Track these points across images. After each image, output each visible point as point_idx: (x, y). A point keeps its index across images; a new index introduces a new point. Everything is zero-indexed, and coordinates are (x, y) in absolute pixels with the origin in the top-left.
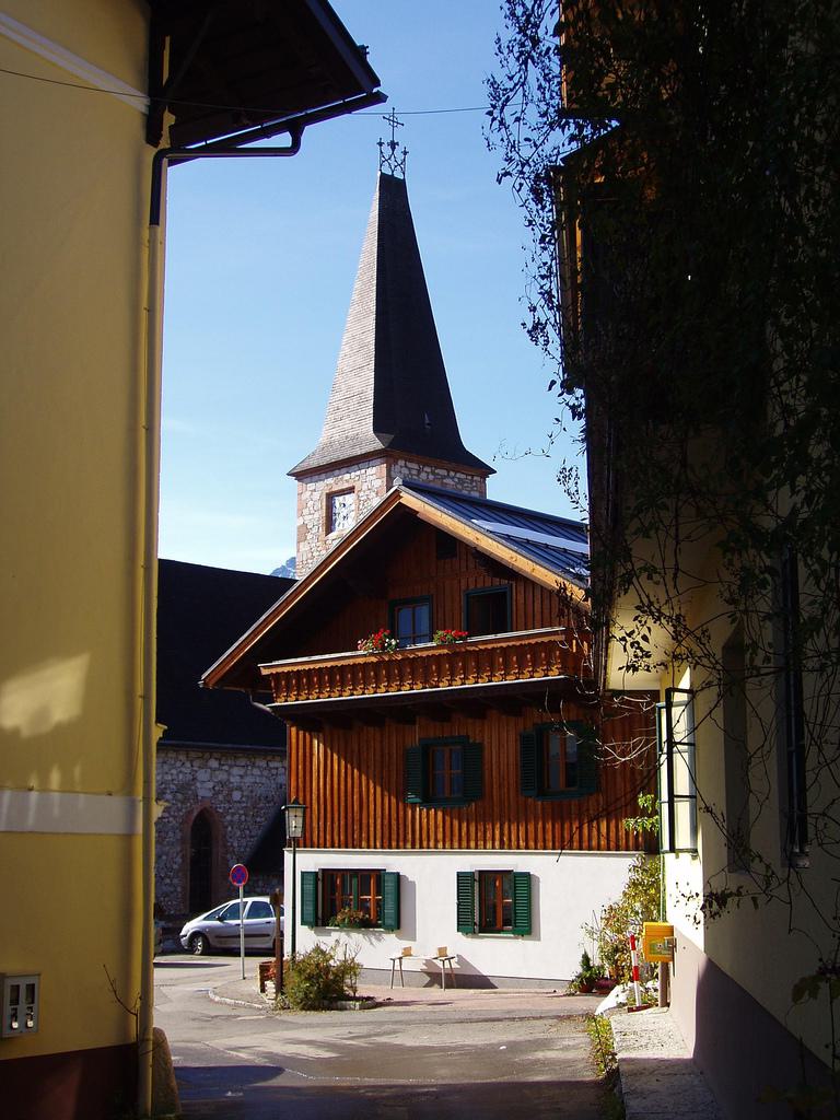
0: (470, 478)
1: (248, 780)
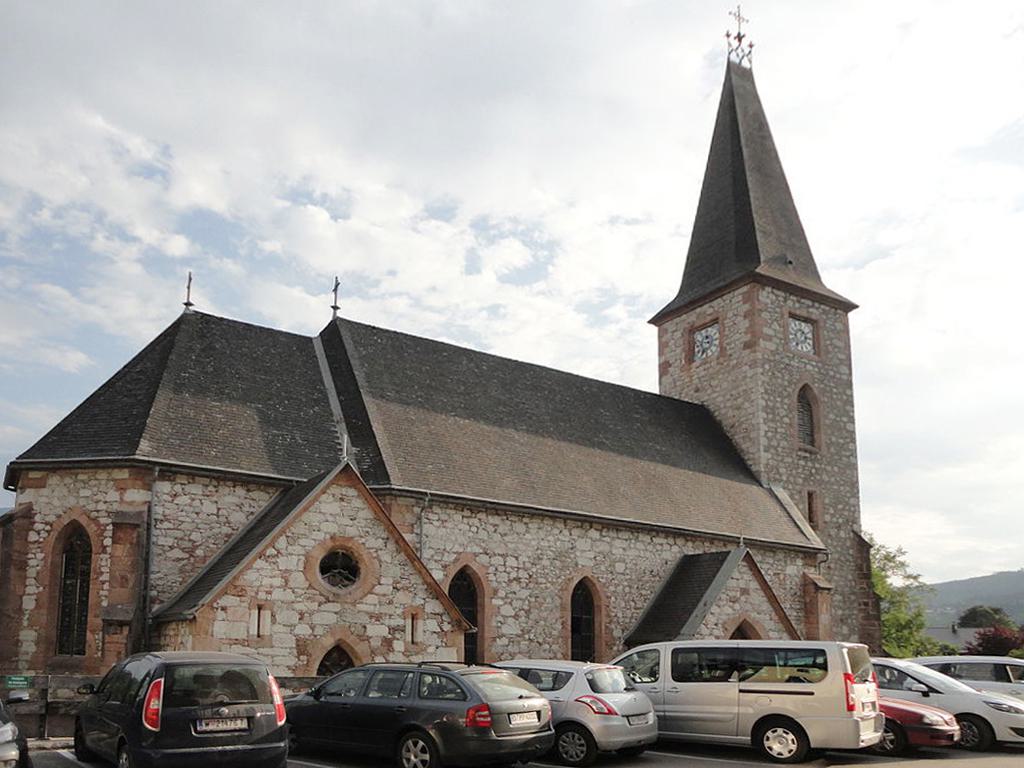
0: (833, 310)
1: (632, 553)
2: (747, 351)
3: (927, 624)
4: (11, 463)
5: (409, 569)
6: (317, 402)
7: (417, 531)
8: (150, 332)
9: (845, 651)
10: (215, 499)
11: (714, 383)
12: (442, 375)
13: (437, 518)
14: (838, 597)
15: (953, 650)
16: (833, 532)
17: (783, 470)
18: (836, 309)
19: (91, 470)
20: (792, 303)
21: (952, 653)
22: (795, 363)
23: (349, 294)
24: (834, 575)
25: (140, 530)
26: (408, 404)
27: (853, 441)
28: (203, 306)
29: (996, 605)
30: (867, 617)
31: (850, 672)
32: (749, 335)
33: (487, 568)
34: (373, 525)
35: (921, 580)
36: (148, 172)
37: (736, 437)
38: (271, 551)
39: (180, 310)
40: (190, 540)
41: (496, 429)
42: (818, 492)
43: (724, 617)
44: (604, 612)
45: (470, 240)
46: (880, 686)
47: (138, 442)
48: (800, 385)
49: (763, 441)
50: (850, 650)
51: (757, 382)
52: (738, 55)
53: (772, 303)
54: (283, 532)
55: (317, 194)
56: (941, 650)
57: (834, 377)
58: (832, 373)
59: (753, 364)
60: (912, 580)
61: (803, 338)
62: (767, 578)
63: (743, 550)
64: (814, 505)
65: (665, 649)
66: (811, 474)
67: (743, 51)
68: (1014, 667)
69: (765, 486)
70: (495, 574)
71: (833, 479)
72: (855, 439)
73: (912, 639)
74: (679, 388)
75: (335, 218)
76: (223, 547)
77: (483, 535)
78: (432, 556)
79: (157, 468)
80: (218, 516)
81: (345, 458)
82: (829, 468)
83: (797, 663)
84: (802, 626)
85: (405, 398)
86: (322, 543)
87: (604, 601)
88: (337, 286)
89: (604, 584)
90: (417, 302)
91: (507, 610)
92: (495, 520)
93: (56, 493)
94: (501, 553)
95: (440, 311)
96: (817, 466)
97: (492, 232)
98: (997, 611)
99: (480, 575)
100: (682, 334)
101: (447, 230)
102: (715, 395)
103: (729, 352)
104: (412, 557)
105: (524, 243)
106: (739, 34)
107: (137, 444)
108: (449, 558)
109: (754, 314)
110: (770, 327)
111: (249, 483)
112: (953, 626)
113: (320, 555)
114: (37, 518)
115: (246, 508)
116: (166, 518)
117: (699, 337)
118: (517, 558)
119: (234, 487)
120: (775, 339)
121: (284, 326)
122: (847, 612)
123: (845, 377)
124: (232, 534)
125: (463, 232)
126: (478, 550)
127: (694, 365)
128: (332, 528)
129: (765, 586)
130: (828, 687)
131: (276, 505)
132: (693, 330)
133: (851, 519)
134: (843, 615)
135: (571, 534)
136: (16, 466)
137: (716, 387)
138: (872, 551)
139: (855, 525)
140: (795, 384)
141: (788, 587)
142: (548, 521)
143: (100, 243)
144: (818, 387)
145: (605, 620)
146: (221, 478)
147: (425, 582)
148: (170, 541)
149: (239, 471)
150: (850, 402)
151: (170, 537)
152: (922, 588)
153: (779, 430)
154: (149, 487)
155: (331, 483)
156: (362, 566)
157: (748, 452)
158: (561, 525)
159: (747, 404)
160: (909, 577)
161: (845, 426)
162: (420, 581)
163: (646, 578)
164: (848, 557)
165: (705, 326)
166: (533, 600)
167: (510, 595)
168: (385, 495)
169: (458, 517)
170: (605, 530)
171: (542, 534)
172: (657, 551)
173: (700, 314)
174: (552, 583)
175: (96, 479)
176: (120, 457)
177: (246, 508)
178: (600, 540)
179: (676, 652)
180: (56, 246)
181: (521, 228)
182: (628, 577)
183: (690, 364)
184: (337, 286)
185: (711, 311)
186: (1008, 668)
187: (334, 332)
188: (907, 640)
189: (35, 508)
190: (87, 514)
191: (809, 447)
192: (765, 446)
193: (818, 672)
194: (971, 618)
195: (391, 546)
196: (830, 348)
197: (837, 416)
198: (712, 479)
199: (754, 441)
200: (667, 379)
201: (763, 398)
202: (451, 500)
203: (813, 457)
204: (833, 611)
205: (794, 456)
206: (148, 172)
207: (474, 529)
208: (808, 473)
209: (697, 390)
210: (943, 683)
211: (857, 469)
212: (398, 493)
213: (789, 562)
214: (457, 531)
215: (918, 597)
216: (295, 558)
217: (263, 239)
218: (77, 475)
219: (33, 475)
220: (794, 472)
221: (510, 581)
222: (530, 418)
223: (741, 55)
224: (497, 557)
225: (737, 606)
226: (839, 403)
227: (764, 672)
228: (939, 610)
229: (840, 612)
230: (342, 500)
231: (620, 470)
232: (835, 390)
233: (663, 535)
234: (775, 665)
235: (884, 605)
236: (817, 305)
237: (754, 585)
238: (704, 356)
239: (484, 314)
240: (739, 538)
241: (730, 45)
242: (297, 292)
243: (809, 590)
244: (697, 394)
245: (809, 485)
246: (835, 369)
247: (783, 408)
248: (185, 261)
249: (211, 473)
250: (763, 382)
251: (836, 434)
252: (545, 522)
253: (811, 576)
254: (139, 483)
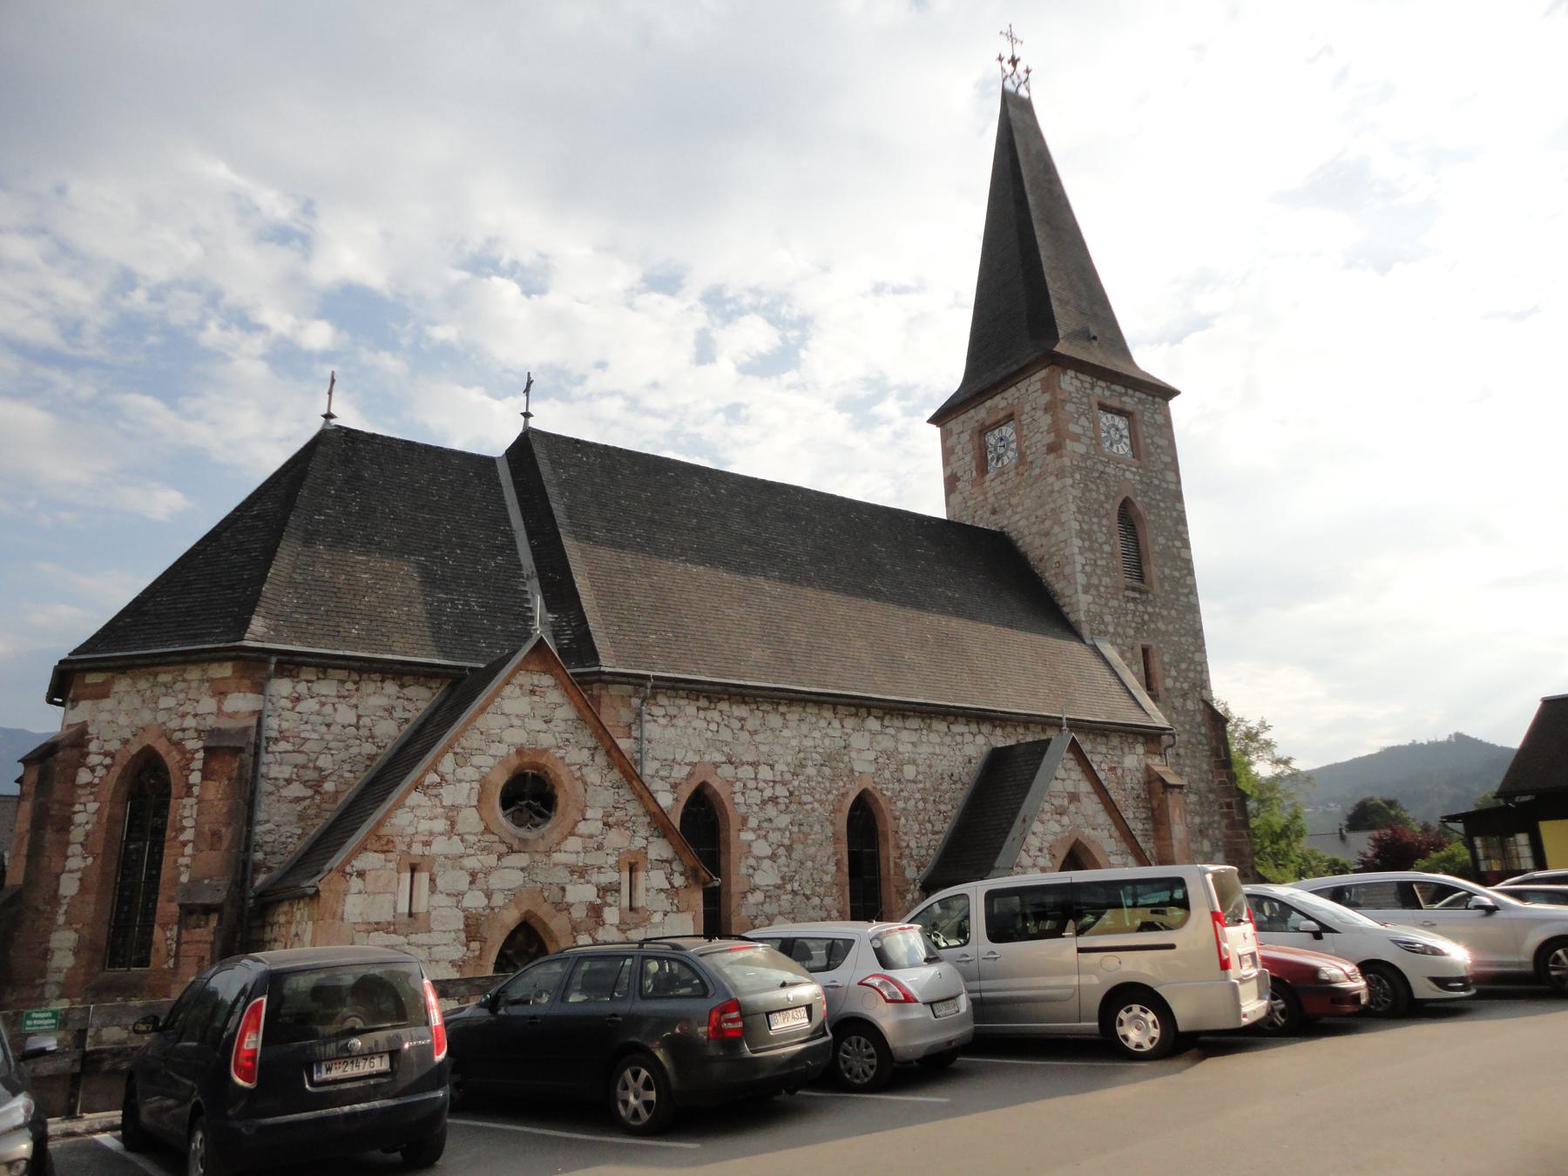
0: (1150, 398)
1: (924, 750)
2: (1051, 457)
3: (1308, 829)
4: (61, 662)
5: (625, 793)
6: (501, 550)
7: (635, 734)
8: (274, 458)
9: (1209, 877)
10: (354, 701)
11: (1014, 501)
12: (669, 504)
13: (663, 713)
14: (1193, 798)
15: (1344, 865)
16: (1178, 703)
17: (1108, 618)
18: (1154, 397)
19: (178, 667)
20: (1101, 391)
21: (1343, 870)
22: (1110, 470)
23: (545, 396)
24: (1185, 765)
25: (244, 756)
26: (623, 548)
27: (1191, 572)
28: (349, 418)
29: (1389, 795)
30: (1232, 825)
31: (1218, 909)
32: (1052, 434)
33: (732, 784)
34: (576, 728)
35: (1295, 765)
36: (283, 236)
37: (1047, 574)
38: (432, 778)
39: (315, 426)
40: (316, 768)
41: (739, 578)
42: (1154, 647)
43: (1050, 838)
44: (891, 842)
45: (700, 318)
46: (1260, 927)
47: (250, 619)
48: (1120, 500)
49: (1081, 579)
50: (1216, 875)
51: (1068, 496)
52: (1013, 82)
53: (1077, 391)
54: (450, 746)
55: (505, 261)
56: (1329, 867)
57: (1158, 487)
58: (1156, 482)
59: (1060, 474)
60: (1282, 766)
61: (1118, 436)
62: (1101, 776)
63: (1068, 736)
64: (1151, 666)
65: (976, 892)
66: (1144, 622)
67: (1019, 77)
68: (1424, 885)
69: (1088, 642)
70: (743, 794)
71: (1170, 628)
72: (1193, 569)
73: (1291, 853)
74: (970, 510)
75: (528, 291)
76: (363, 776)
77: (726, 735)
78: (657, 771)
79: (274, 659)
80: (358, 728)
81: (538, 630)
82: (1165, 613)
83: (1151, 901)
84: (1151, 845)
85: (618, 539)
86: (503, 761)
87: (891, 825)
88: (529, 385)
89: (890, 798)
90: (633, 404)
91: (761, 848)
92: (740, 711)
93: (124, 706)
94: (750, 760)
95: (663, 415)
96: (1150, 609)
97: (729, 307)
98: (1391, 804)
99: (722, 796)
100: (971, 437)
101: (670, 306)
102: (1017, 517)
103: (1029, 459)
104: (628, 772)
105: (771, 322)
106: (1013, 58)
107: (245, 624)
108: (680, 773)
109: (1056, 407)
110: (1077, 423)
111: (404, 674)
112: (1340, 830)
113: (500, 779)
114: (93, 747)
115: (398, 714)
116: (283, 736)
117: (991, 439)
118: (772, 767)
119: (382, 681)
120: (1084, 440)
121: (457, 444)
122: (1206, 819)
123: (1172, 487)
124: (376, 755)
125: (691, 309)
126: (719, 757)
127: (988, 477)
128: (517, 737)
129: (1100, 789)
130: (1193, 934)
131: (442, 703)
132: (984, 430)
133: (1199, 683)
134: (1202, 823)
135: (843, 726)
136: (69, 667)
137: (1017, 506)
138: (1230, 728)
139: (1204, 691)
140: (1114, 498)
141: (1128, 786)
142: (811, 709)
143: (213, 334)
144: (1142, 501)
145: (893, 854)
146: (364, 669)
147: (648, 812)
148: (287, 771)
149: (390, 657)
150: (1181, 520)
151: (287, 764)
152: (1295, 776)
153: (1099, 562)
154: (259, 688)
155: (519, 668)
156: (560, 794)
157: (1063, 595)
158: (828, 714)
159: (1057, 529)
160: (1278, 762)
161: (1179, 553)
162: (641, 811)
163: (945, 786)
164: (1199, 737)
165: (998, 424)
166: (795, 829)
167: (765, 825)
168: (592, 683)
169: (690, 709)
170: (887, 717)
171: (805, 728)
172: (957, 744)
173: (990, 408)
174: (821, 802)
175: (184, 681)
176: (221, 645)
177: (398, 714)
178: (882, 733)
179: (991, 896)
180: (151, 340)
181: (765, 301)
182: (921, 786)
183: (983, 476)
184: (529, 385)
185: (1003, 404)
186: (1415, 886)
187: (527, 446)
188: (1286, 855)
189: (90, 730)
190: (167, 735)
191: (1137, 584)
192: (1083, 585)
193: (1177, 913)
194: (1363, 816)
195: (601, 759)
196: (1152, 449)
197: (1167, 540)
198: (1019, 637)
199: (1069, 580)
200: (957, 498)
201: (1075, 520)
202: (682, 685)
203: (1144, 597)
204: (1189, 818)
205: (1121, 597)
206: (283, 236)
207: (713, 727)
208: (1139, 620)
209: (994, 512)
210: (1337, 917)
211: (1199, 613)
212: (610, 678)
213: (1126, 750)
214: (690, 731)
215: (1292, 790)
216: (466, 786)
217: (434, 323)
218: (156, 675)
219: (92, 679)
220: (1122, 619)
221: (764, 802)
222: (784, 560)
223: (1017, 82)
224: (746, 767)
225: (1065, 820)
226: (1169, 522)
227: (1108, 917)
228: (1321, 808)
229: (1197, 820)
230: (533, 692)
231: (903, 629)
232: (1162, 505)
233: (964, 719)
234: (1120, 906)
235: (1252, 805)
236: (1130, 392)
237: (1085, 787)
238: (1000, 465)
239: (721, 417)
240: (1061, 718)
241: (1003, 70)
242: (476, 395)
243: (1155, 786)
244: (995, 517)
245: (1143, 637)
246: (1159, 476)
247: (1101, 532)
248: (327, 356)
249: (351, 663)
250: (1074, 497)
251: (1169, 564)
252: (808, 710)
253: (1156, 769)
254: (247, 682)
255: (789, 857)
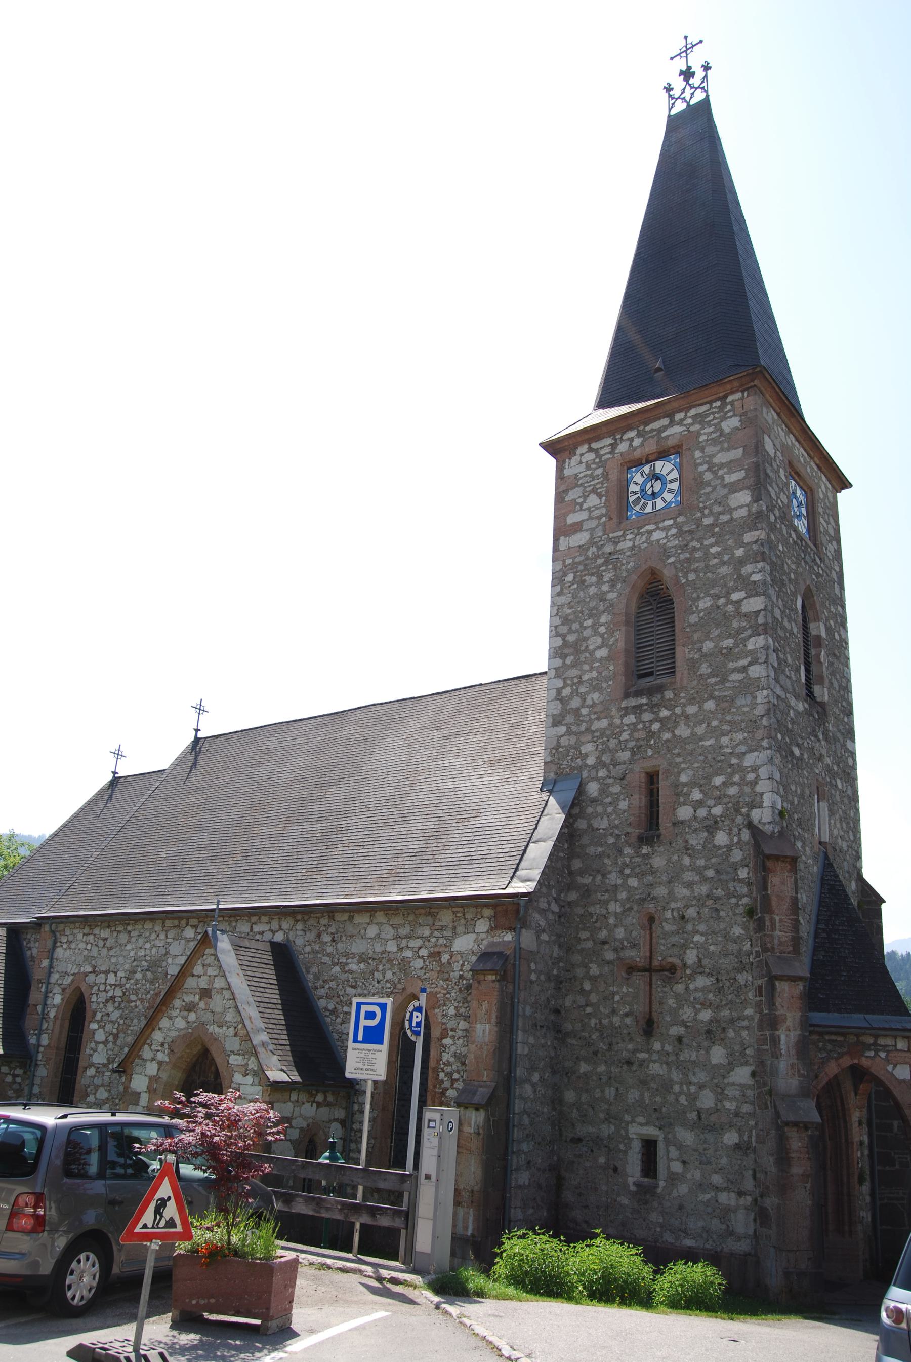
33: (92, 987)
70: (97, 994)
94: (104, 969)
118: (116, 973)
126: (89, 969)
135: (167, 937)
167: (105, 1018)
174: (142, 1000)
255: (114, 1043)
